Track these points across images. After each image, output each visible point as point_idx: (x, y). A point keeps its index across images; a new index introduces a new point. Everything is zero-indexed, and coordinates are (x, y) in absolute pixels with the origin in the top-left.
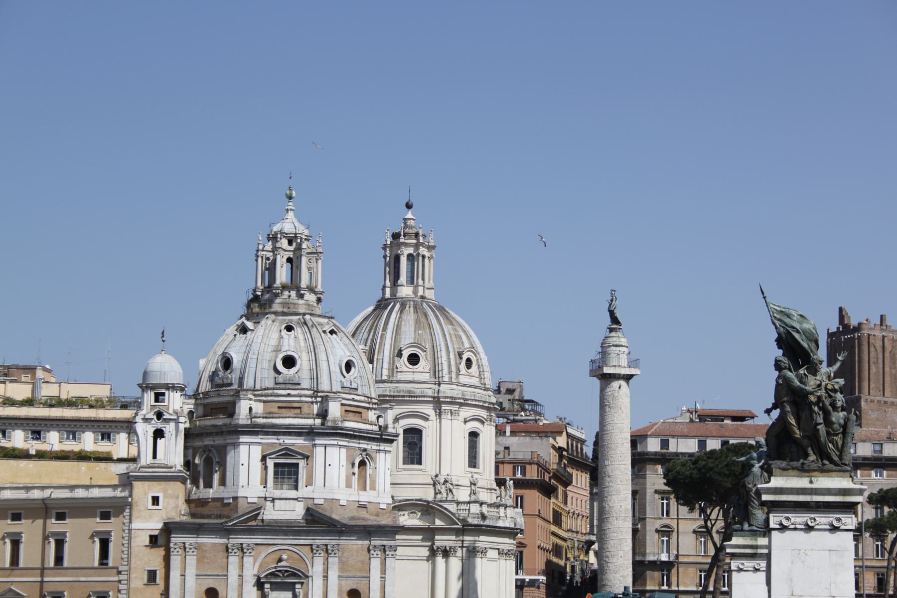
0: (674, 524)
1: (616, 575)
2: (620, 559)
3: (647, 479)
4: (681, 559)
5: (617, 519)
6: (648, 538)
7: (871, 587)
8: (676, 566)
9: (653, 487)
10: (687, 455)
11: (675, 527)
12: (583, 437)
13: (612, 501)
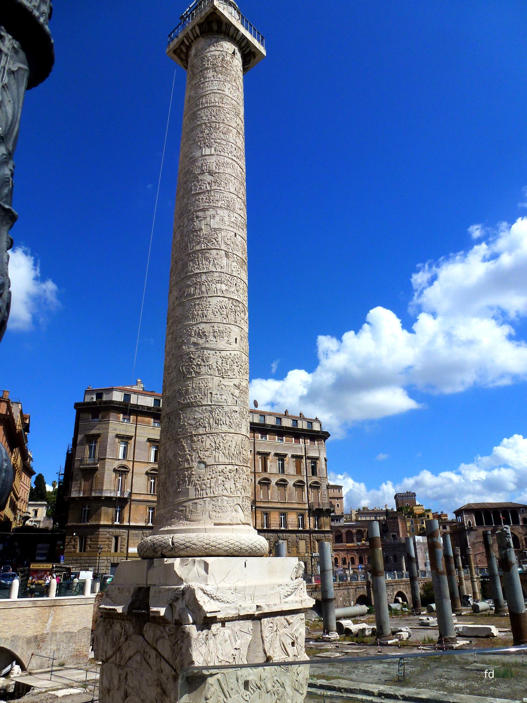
0: (130, 465)
1: (225, 382)
2: (234, 346)
3: (110, 425)
4: (134, 497)
5: (227, 255)
6: (106, 476)
7: (277, 524)
8: (129, 503)
9: (114, 431)
10: (146, 408)
11: (131, 468)
12: (31, 456)
13: (217, 218)
